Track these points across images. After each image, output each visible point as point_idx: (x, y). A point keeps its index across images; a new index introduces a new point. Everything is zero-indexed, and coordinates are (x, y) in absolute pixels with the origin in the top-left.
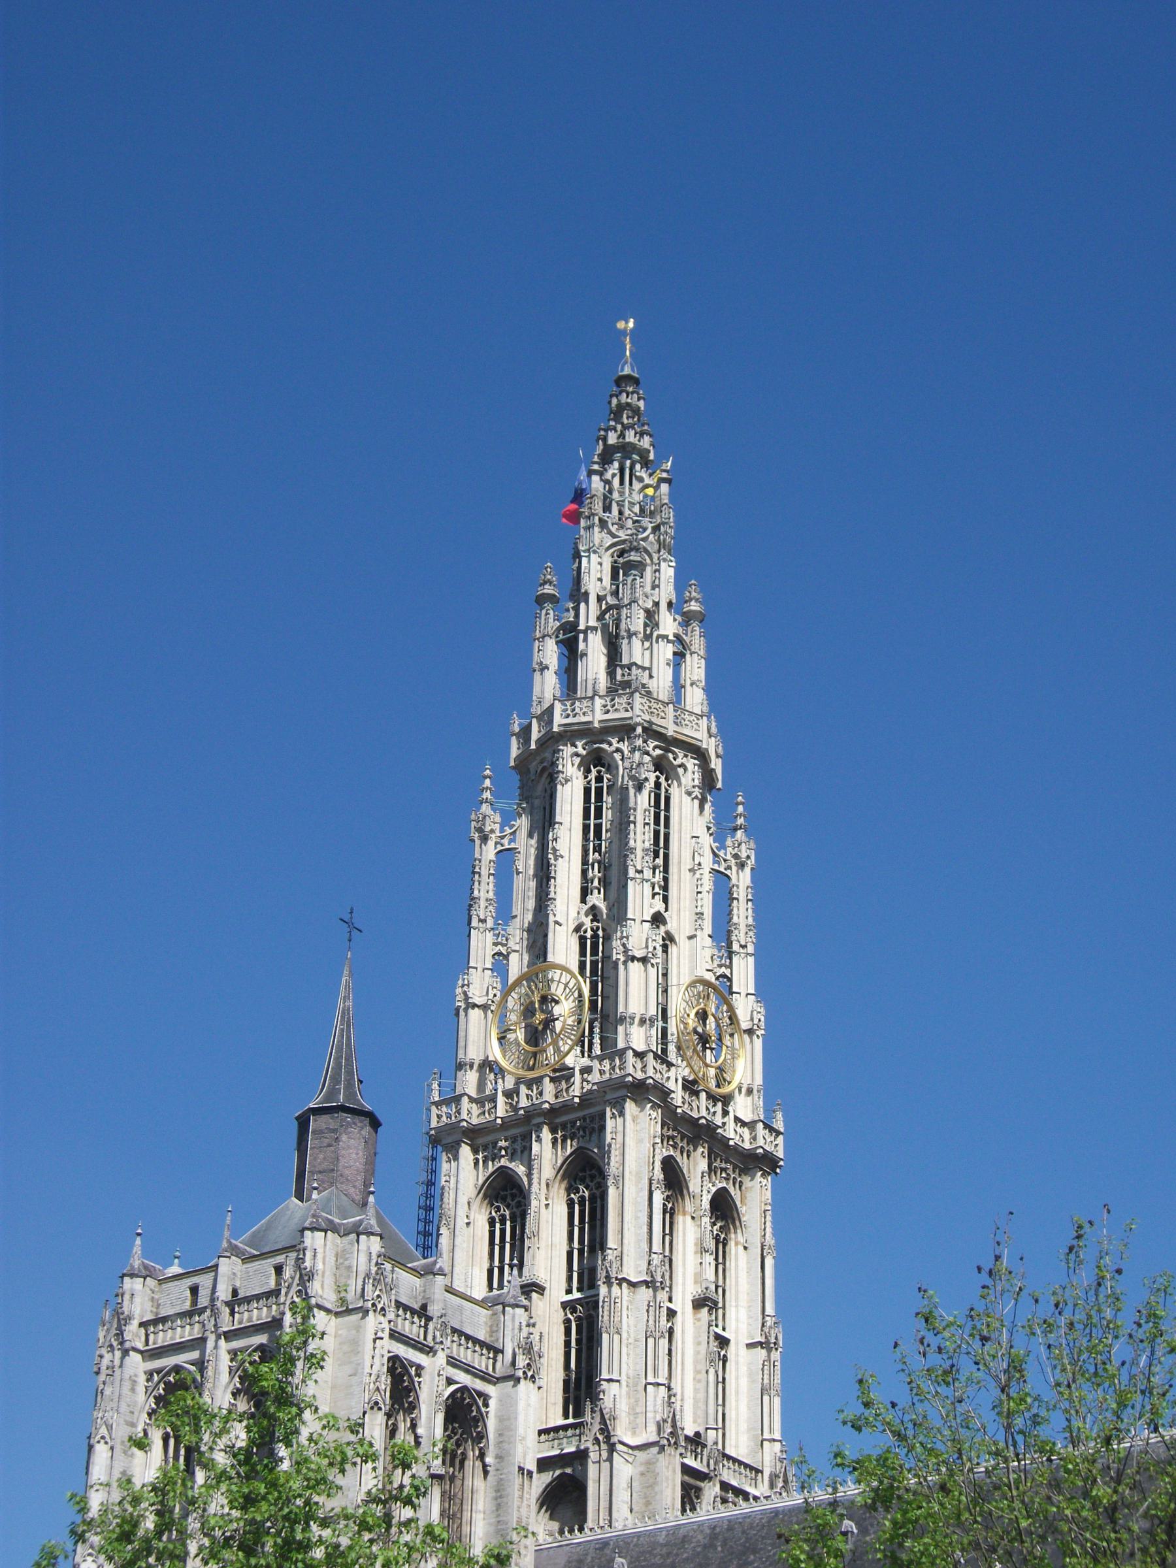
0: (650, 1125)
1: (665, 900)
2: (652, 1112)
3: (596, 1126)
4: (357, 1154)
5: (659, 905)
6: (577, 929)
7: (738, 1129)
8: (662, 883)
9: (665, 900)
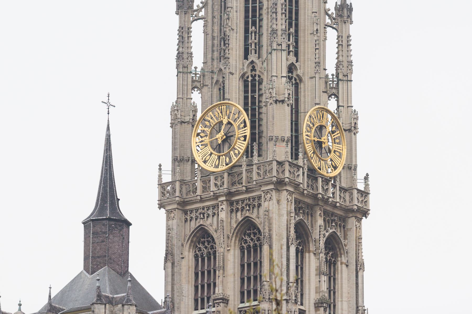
0: (287, 205)
1: (296, 55)
2: (288, 197)
3: (256, 204)
4: (119, 246)
5: (292, 59)
6: (243, 76)
7: (342, 195)
8: (294, 44)
9: (296, 55)
